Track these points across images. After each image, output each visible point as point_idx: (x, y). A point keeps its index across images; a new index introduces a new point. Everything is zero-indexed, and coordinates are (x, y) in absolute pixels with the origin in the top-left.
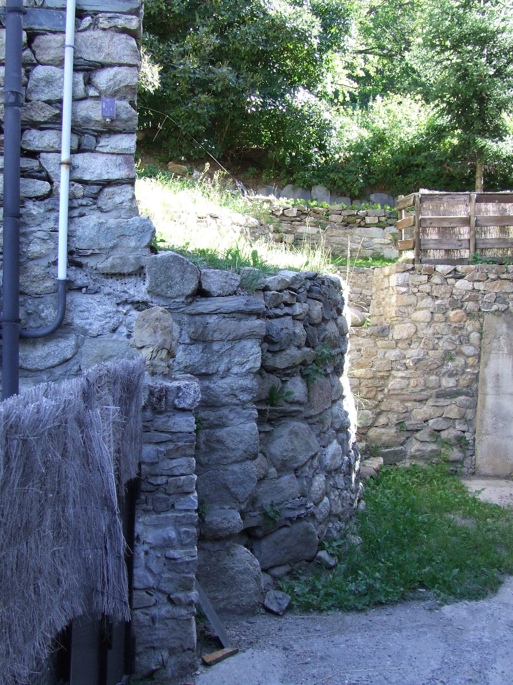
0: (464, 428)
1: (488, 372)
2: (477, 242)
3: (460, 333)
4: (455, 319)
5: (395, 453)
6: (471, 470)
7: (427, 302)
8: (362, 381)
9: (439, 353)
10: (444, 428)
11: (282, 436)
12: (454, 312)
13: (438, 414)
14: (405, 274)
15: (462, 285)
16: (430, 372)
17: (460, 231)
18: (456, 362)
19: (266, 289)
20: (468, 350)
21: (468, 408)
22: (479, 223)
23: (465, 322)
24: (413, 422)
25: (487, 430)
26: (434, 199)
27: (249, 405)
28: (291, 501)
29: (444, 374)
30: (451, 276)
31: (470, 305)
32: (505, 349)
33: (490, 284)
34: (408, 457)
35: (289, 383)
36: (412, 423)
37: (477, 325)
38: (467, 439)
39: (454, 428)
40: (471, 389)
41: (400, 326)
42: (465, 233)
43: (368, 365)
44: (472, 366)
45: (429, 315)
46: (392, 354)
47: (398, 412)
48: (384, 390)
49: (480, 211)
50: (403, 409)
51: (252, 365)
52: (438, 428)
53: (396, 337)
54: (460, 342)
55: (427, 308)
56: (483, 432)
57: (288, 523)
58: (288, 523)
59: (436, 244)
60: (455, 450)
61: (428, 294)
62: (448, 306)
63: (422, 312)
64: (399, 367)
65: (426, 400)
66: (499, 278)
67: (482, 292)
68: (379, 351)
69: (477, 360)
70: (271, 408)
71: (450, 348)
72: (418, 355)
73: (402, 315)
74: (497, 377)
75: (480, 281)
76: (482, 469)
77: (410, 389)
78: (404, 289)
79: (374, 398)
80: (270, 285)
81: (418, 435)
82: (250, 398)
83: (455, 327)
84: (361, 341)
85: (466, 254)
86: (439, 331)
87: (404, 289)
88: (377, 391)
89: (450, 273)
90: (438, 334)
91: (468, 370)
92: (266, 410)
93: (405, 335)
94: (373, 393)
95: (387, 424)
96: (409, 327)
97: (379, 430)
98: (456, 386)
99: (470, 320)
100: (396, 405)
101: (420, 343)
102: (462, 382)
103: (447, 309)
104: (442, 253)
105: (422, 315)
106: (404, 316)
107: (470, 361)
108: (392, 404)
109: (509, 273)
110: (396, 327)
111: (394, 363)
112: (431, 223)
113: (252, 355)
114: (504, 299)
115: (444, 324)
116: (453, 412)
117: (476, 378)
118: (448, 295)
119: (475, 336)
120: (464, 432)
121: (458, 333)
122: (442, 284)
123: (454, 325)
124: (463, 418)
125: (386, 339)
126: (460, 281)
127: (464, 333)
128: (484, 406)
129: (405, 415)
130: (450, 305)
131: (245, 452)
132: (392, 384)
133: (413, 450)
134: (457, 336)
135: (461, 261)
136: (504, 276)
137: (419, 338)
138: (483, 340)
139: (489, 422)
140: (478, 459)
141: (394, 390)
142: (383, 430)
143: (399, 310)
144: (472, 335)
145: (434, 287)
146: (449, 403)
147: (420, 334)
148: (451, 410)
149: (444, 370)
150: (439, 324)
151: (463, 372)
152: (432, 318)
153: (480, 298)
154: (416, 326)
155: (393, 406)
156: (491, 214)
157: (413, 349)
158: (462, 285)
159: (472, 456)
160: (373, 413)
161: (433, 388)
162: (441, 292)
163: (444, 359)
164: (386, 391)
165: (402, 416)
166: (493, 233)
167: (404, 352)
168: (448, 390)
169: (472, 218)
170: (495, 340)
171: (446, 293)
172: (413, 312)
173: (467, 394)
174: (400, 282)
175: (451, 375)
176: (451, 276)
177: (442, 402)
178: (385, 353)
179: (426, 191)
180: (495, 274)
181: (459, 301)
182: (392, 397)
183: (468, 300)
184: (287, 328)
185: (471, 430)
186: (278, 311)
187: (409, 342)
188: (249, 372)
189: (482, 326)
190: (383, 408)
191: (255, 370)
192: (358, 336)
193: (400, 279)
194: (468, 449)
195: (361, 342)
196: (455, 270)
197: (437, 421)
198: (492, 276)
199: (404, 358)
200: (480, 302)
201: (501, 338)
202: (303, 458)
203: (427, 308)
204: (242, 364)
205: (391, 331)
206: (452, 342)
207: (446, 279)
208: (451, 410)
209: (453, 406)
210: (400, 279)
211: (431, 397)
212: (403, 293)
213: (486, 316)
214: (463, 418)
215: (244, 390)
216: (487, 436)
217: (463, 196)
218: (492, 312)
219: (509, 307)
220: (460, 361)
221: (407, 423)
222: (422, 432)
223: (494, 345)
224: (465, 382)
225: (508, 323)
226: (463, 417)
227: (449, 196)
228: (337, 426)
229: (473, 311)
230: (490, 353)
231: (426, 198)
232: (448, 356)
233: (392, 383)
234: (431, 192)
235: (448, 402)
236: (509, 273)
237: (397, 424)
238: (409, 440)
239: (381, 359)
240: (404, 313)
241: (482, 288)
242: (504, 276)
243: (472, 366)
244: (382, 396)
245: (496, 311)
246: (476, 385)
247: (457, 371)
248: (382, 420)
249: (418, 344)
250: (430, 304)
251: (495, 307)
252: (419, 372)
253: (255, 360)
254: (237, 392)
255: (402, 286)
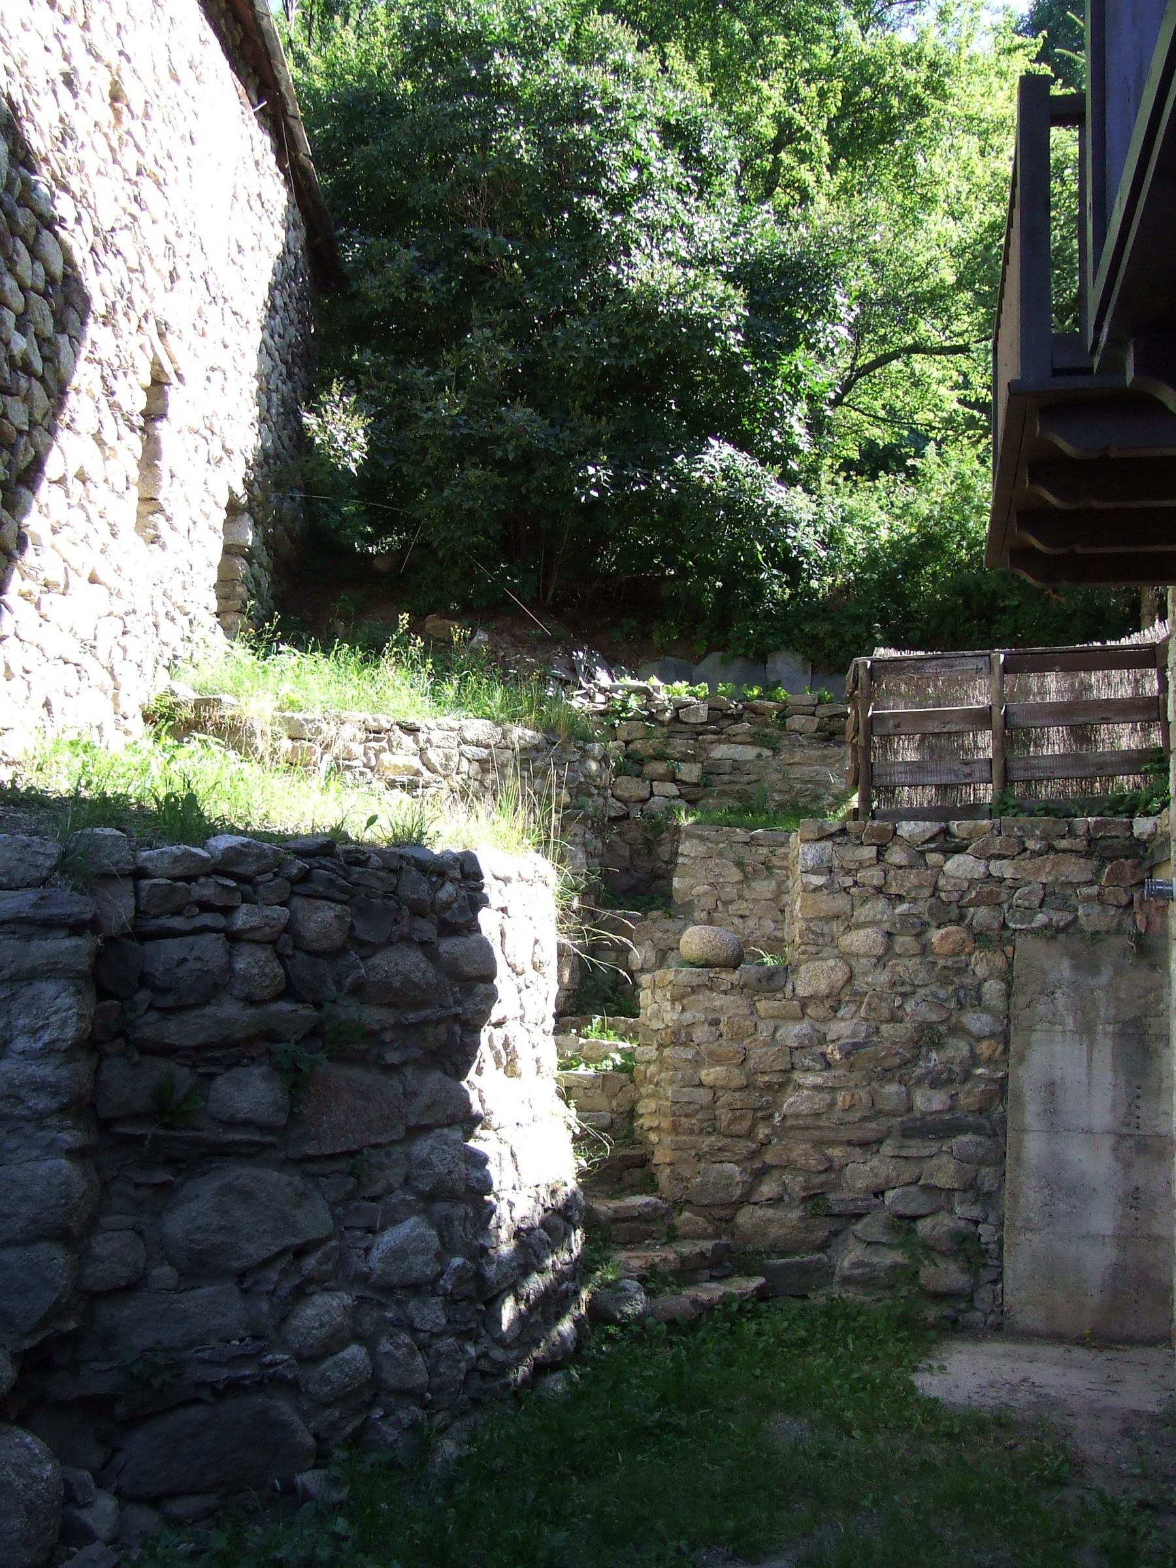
0: (975, 1212)
1: (1028, 1077)
2: (1010, 764)
3: (957, 981)
4: (946, 948)
5: (803, 1269)
6: (991, 1318)
7: (877, 908)
8: (719, 1094)
9: (905, 1029)
10: (922, 1211)
11: (197, 1196)
12: (943, 931)
13: (906, 1178)
14: (823, 844)
15: (961, 867)
16: (886, 1075)
17: (975, 742)
18: (950, 1053)
19: (140, 874)
20: (977, 1022)
21: (982, 1163)
22: (1016, 720)
23: (970, 954)
24: (846, 1195)
25: (1029, 1220)
26: (903, 669)
27: (54, 1121)
28: (214, 1343)
29: (919, 1081)
30: (932, 846)
31: (981, 915)
32: (1070, 1020)
33: (1028, 864)
34: (836, 1279)
35: (220, 1081)
36: (843, 1196)
37: (999, 961)
38: (983, 1239)
39: (951, 1211)
40: (989, 1118)
41: (812, 965)
42: (985, 743)
43: (733, 1058)
44: (990, 1061)
45: (880, 938)
46: (792, 1032)
47: (807, 1171)
48: (771, 1116)
49: (1027, 692)
50: (819, 1161)
51: (56, 1034)
52: (908, 1212)
53: (800, 992)
54: (959, 1002)
55: (873, 923)
56: (1018, 1224)
57: (205, 1395)
58: (205, 1395)
59: (911, 772)
60: (953, 1267)
61: (879, 890)
62: (926, 917)
63: (862, 932)
64: (807, 1062)
65: (880, 1142)
66: (1051, 849)
67: (1008, 882)
68: (761, 1026)
69: (1001, 1048)
70: (162, 1132)
71: (934, 1017)
72: (853, 1035)
73: (819, 942)
74: (1051, 1088)
75: (1004, 857)
76: (1019, 1318)
77: (836, 1116)
78: (818, 880)
79: (750, 1134)
80: (149, 865)
81: (858, 1227)
82: (54, 1105)
83: (944, 967)
84: (719, 1000)
85: (986, 793)
86: (906, 977)
87: (818, 880)
88: (755, 1119)
89: (932, 839)
90: (903, 983)
91: (979, 1071)
92: (144, 1137)
93: (823, 987)
94: (745, 1125)
95: (781, 1199)
96: (832, 969)
97: (760, 1212)
98: (951, 1109)
99: (981, 949)
100: (800, 1151)
101: (859, 1007)
102: (964, 1100)
103: (925, 925)
104: (931, 792)
105: (862, 940)
106: (820, 941)
107: (984, 1049)
108: (791, 1150)
109: (1077, 836)
110: (803, 968)
111: (797, 1053)
112: (897, 726)
113: (55, 1013)
114: (1065, 899)
115: (918, 960)
116: (944, 1172)
117: (1001, 1089)
118: (927, 892)
119: (993, 989)
120: (976, 1223)
121: (952, 982)
122: (912, 867)
123: (941, 962)
124: (971, 1187)
125: (779, 996)
126: (957, 859)
127: (968, 980)
128: (1018, 1160)
129: (823, 1178)
130: (931, 914)
131: (33, 1221)
132: (791, 1102)
133: (846, 1264)
134: (951, 989)
135: (973, 811)
136: (1064, 844)
137: (856, 993)
138: (1013, 999)
139: (1032, 1200)
140: (1007, 1290)
141: (797, 1116)
142: (770, 1213)
143: (809, 929)
144: (987, 985)
145: (892, 873)
146: (934, 1150)
147: (860, 984)
148: (940, 1168)
149: (918, 1071)
150: (906, 961)
151: (967, 1076)
152: (889, 948)
153: (1004, 897)
154: (851, 967)
155: (794, 1155)
156: (1052, 698)
157: (843, 1019)
158: (961, 866)
159: (995, 1282)
160: (745, 1170)
161: (893, 1114)
162: (907, 885)
163: (917, 1045)
164: (777, 1118)
165: (817, 1180)
166: (1055, 742)
167: (824, 1028)
168: (929, 1118)
169: (995, 709)
170: (1043, 998)
171: (921, 886)
172: (844, 933)
173: (977, 1130)
174: (810, 863)
175: (936, 1082)
176: (932, 846)
177: (915, 1148)
178: (776, 1029)
179: (892, 653)
180: (1042, 839)
181: (954, 906)
182: (792, 1133)
183: (975, 903)
184: (198, 959)
185: (991, 1219)
186: (177, 922)
187: (834, 1002)
188: (49, 1050)
189: (1010, 966)
190: (769, 1158)
191: (64, 1045)
192: (711, 989)
193: (809, 857)
194: (985, 1265)
195: (717, 1003)
196: (946, 832)
197: (905, 1194)
198: (1032, 845)
199: (823, 1040)
200: (1005, 906)
201: (1058, 994)
202: (255, 1250)
203: (873, 923)
204: (34, 1032)
205: (791, 978)
206: (940, 1004)
207: (922, 854)
208: (940, 1168)
209: (945, 1159)
210: (809, 857)
211: (889, 1133)
212: (817, 889)
213: (1019, 941)
214: (971, 1187)
215: (39, 1087)
216: (1029, 1235)
217: (974, 660)
218: (1036, 932)
219: (1076, 918)
220: (957, 1049)
221: (832, 1197)
222: (866, 1220)
223: (1041, 1009)
224: (970, 1100)
225: (1073, 956)
226: (971, 1187)
227: (940, 662)
228: (425, 1186)
229: (989, 929)
230: (1031, 1029)
231: (885, 668)
232: (928, 1037)
233: (791, 1100)
234: (905, 654)
235: (933, 1148)
236: (1077, 836)
237: (804, 1200)
238: (841, 1237)
239: (765, 1044)
240: (823, 935)
241: (1008, 874)
242: (1064, 844)
243: (990, 1061)
244: (767, 1131)
245: (1045, 927)
246: (1001, 1108)
247: (950, 1071)
248: (768, 1189)
249: (853, 1009)
250: (883, 913)
251: (1040, 919)
252: (857, 1075)
253: (63, 1024)
254: (23, 1092)
255: (814, 872)
